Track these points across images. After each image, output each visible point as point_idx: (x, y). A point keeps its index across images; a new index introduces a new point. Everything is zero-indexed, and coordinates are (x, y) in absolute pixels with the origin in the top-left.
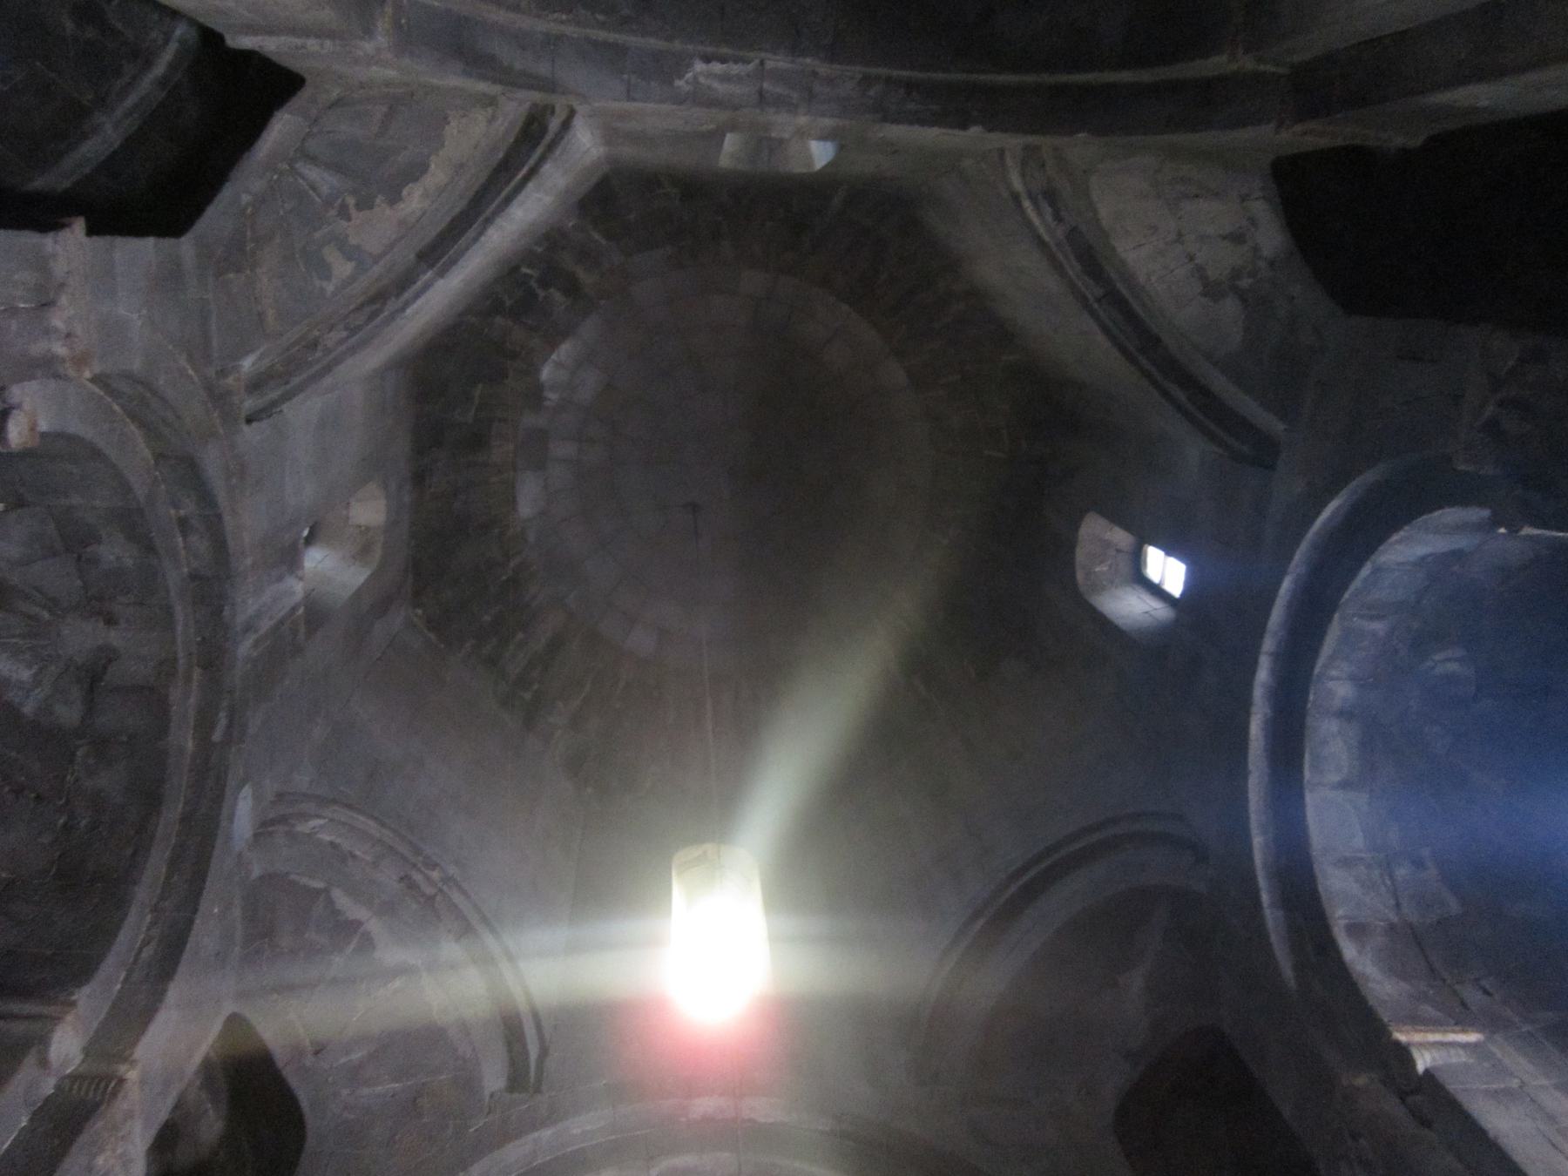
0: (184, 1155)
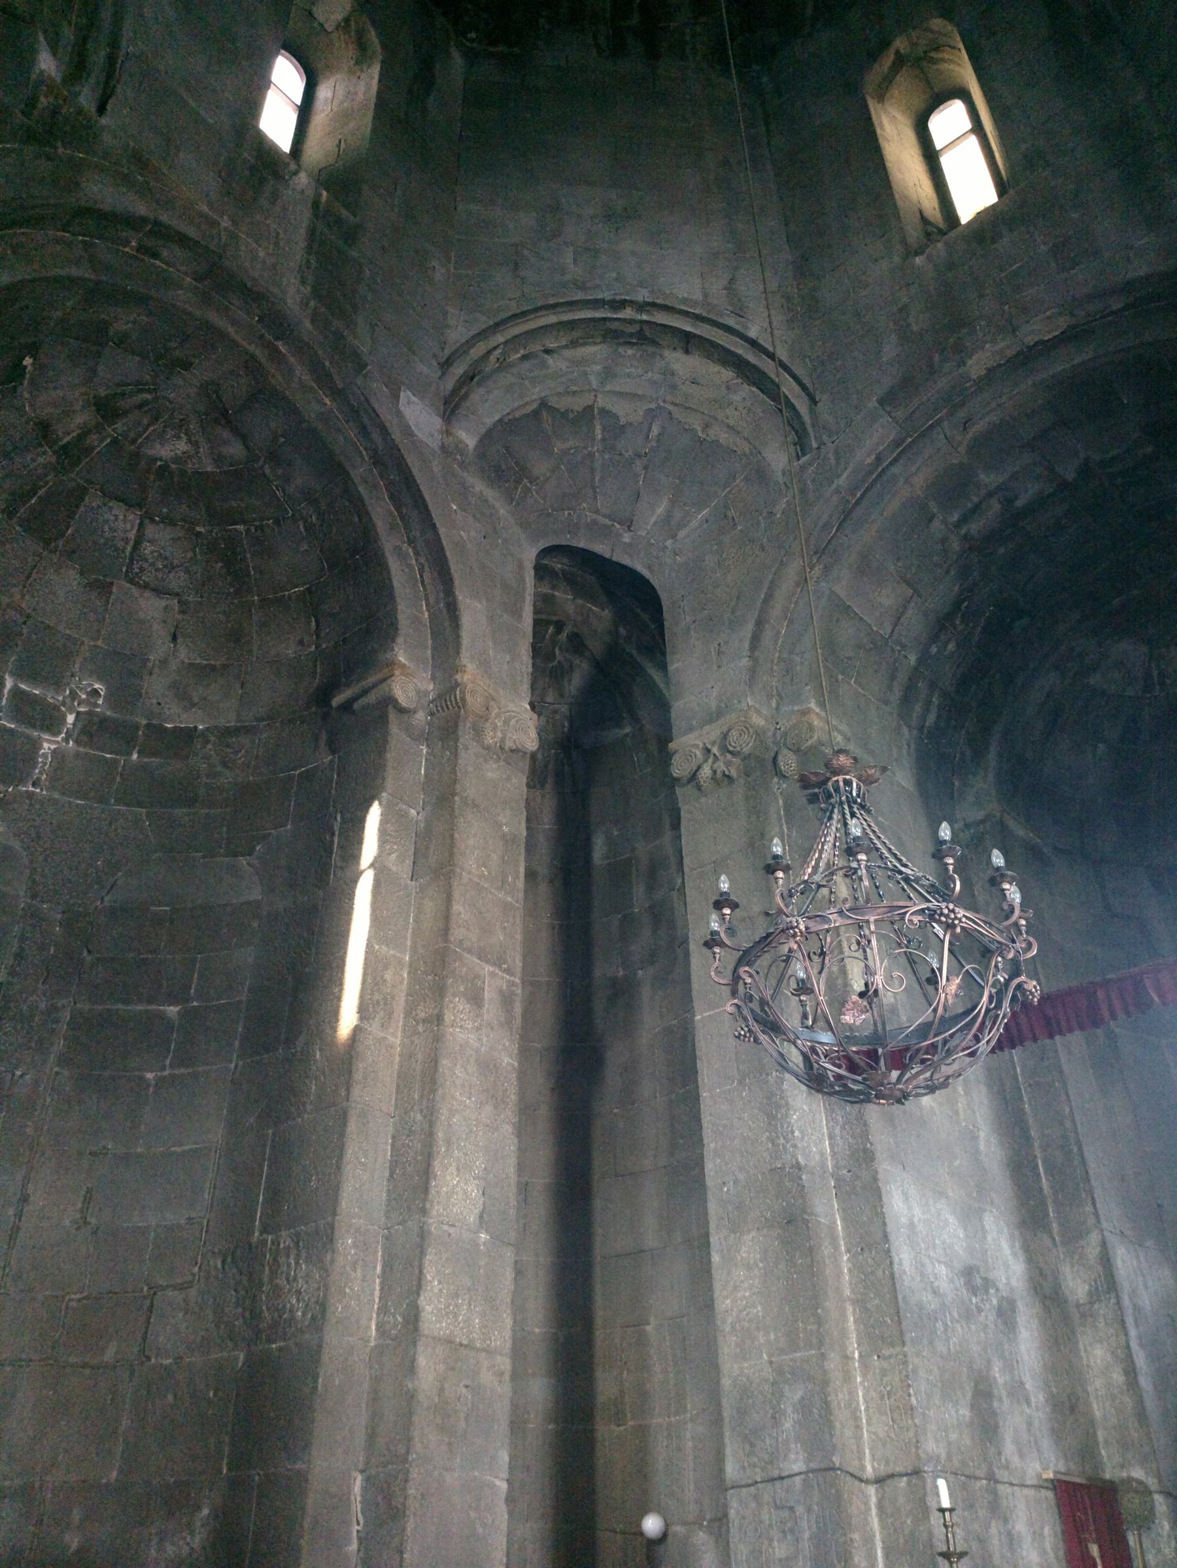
0: (596, 646)
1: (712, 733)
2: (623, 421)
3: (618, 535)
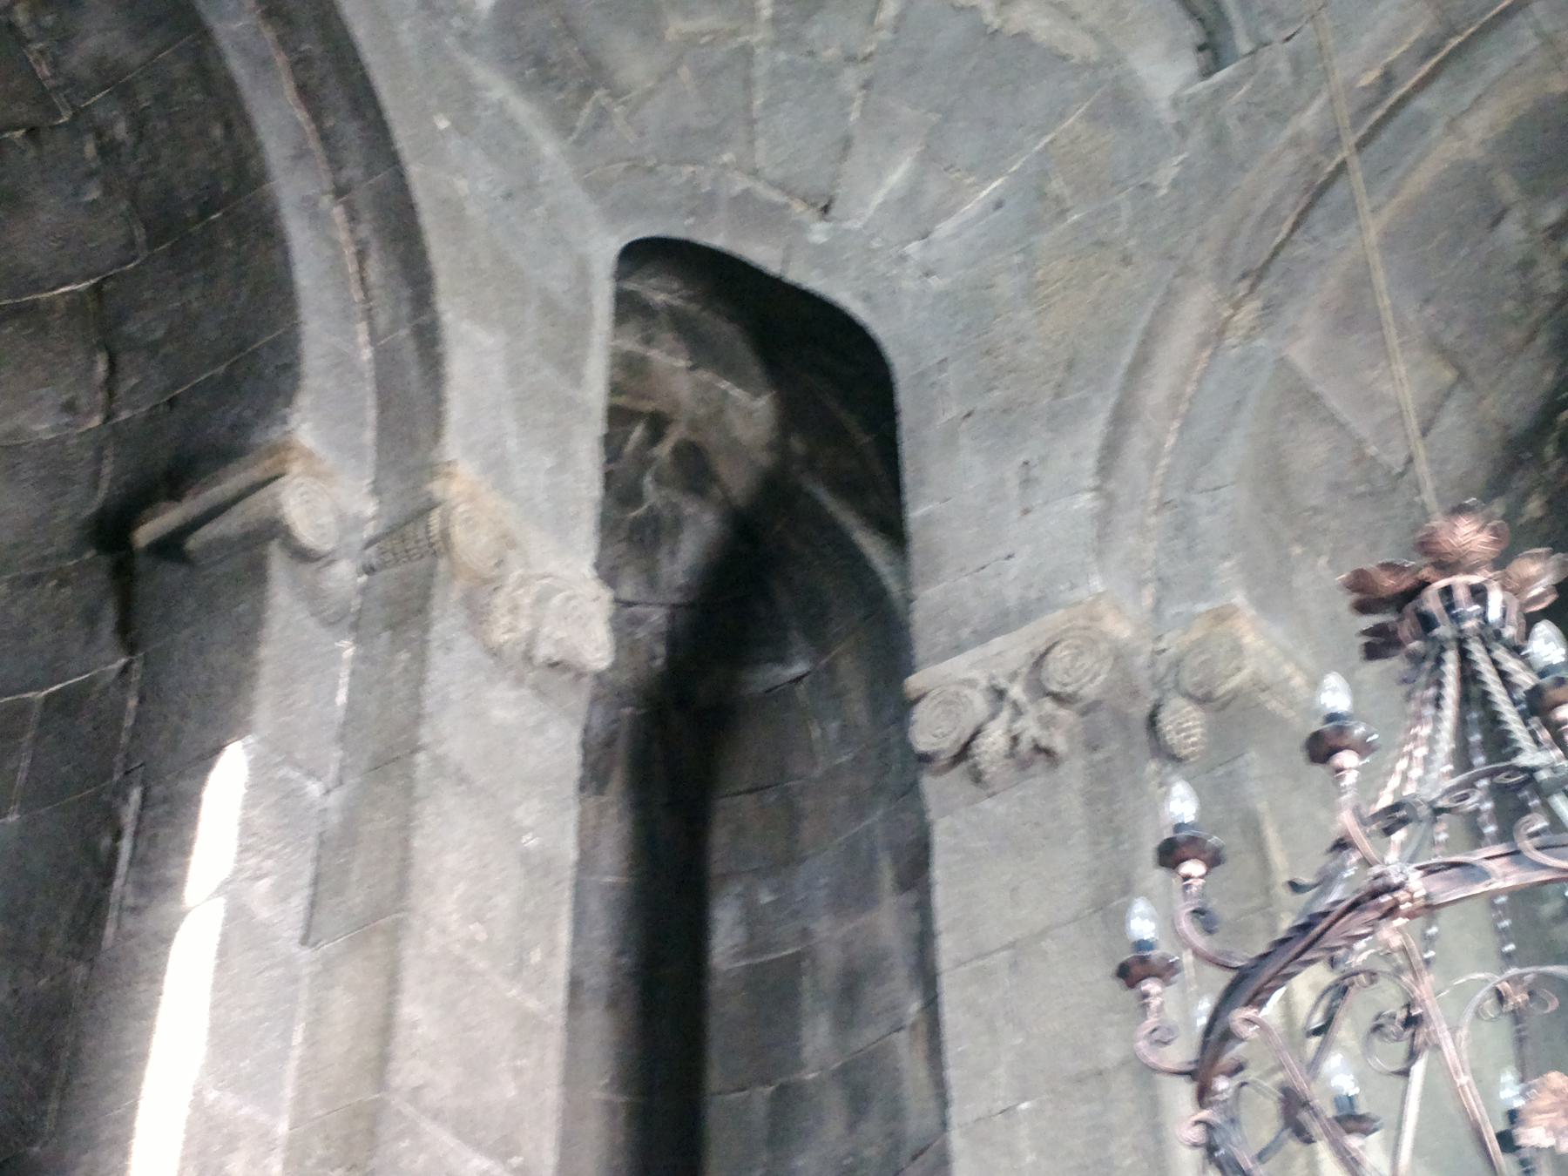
0: (737, 480)
1: (1012, 650)
3: (800, 227)
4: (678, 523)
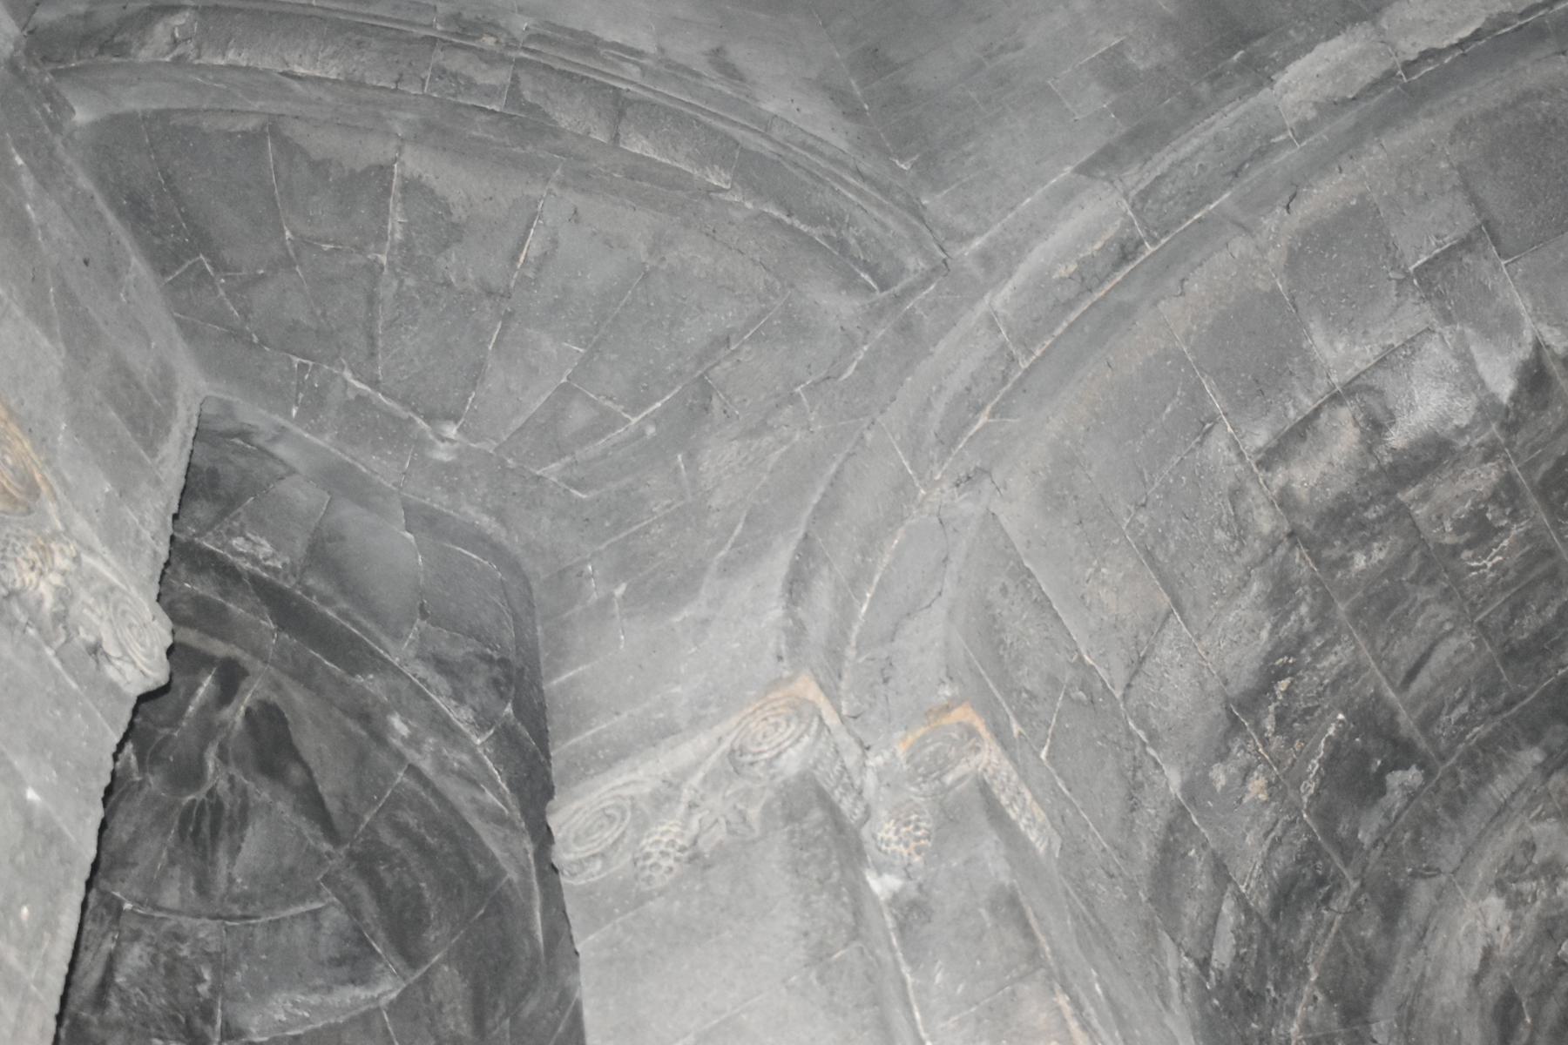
2: (459, 214)
4: (243, 815)
